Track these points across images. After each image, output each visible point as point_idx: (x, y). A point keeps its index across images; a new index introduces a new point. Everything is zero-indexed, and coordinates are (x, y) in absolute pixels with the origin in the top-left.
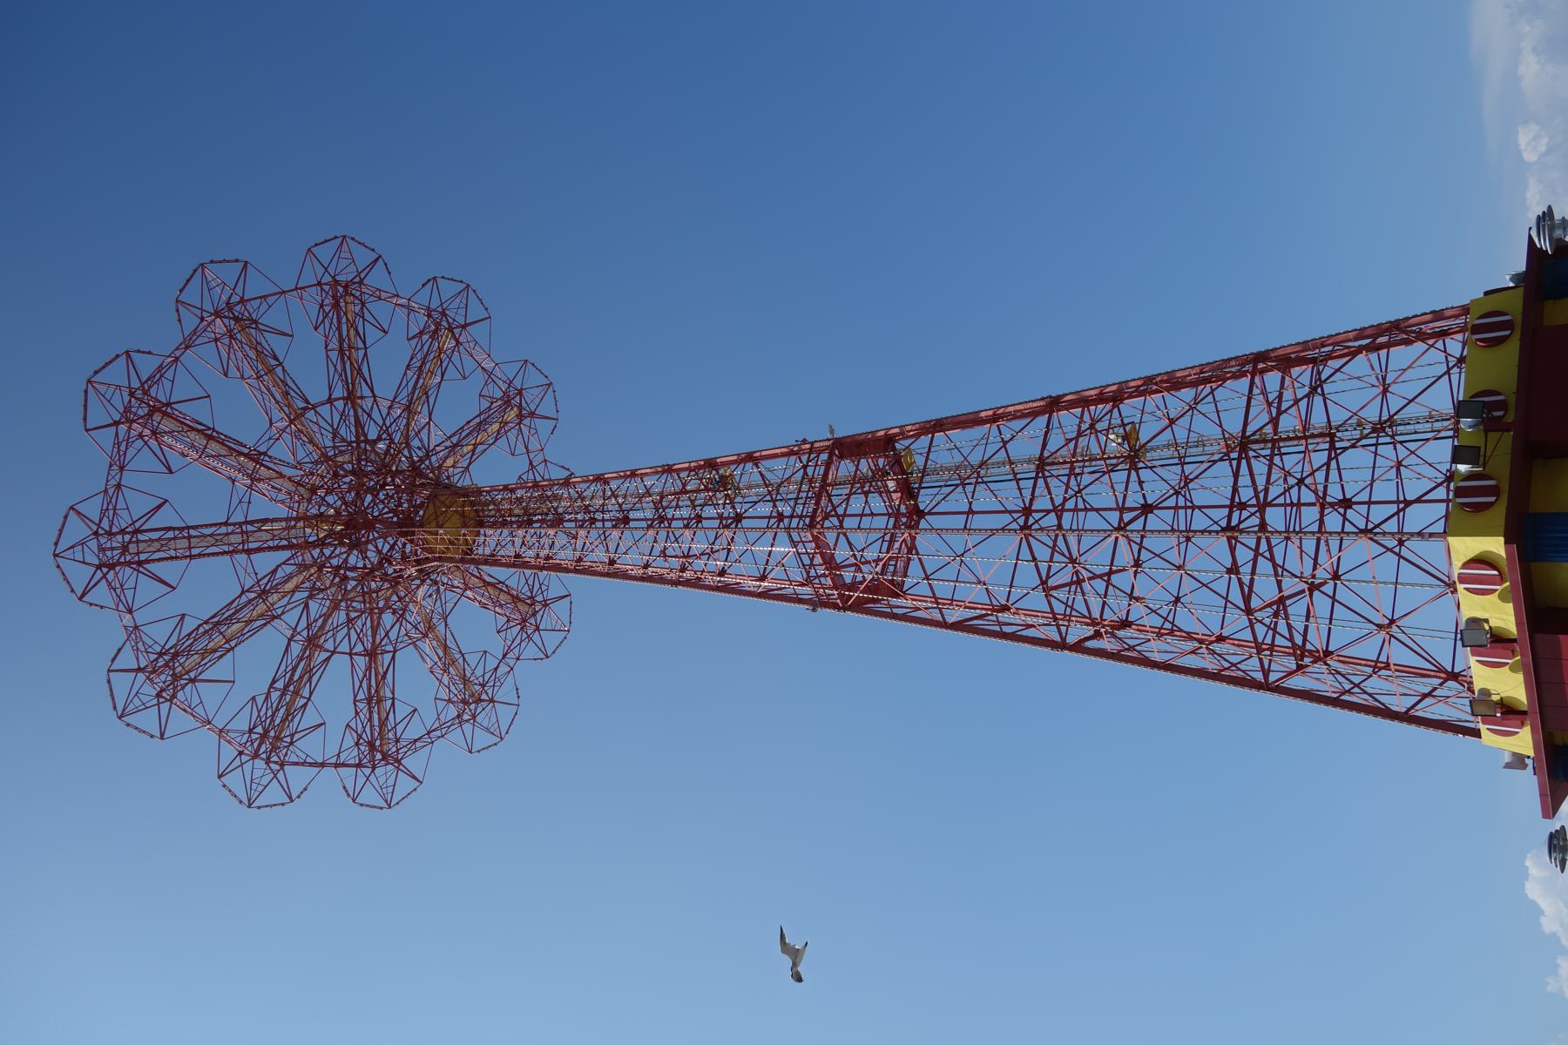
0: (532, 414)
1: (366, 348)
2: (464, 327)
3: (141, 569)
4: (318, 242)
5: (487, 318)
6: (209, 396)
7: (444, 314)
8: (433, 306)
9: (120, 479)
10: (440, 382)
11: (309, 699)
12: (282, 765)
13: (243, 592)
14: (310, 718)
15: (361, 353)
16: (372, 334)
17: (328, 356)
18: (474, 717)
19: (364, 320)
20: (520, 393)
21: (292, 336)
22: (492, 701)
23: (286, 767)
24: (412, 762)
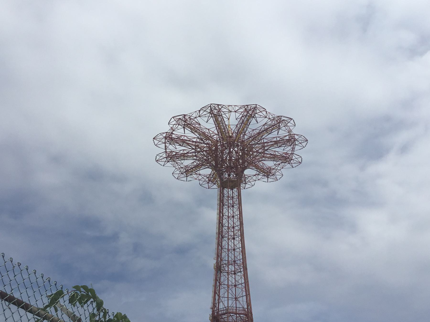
1: (278, 147)
3: (209, 118)
9: (233, 112)
11: (182, 146)
12: (165, 143)
13: (208, 129)
14: (177, 147)
15: (277, 146)
16: (282, 148)
17: (275, 137)
18: (182, 174)
19: (285, 146)
20: (274, 175)
21: (278, 135)
22: (187, 176)
23: (164, 144)
24: (169, 164)
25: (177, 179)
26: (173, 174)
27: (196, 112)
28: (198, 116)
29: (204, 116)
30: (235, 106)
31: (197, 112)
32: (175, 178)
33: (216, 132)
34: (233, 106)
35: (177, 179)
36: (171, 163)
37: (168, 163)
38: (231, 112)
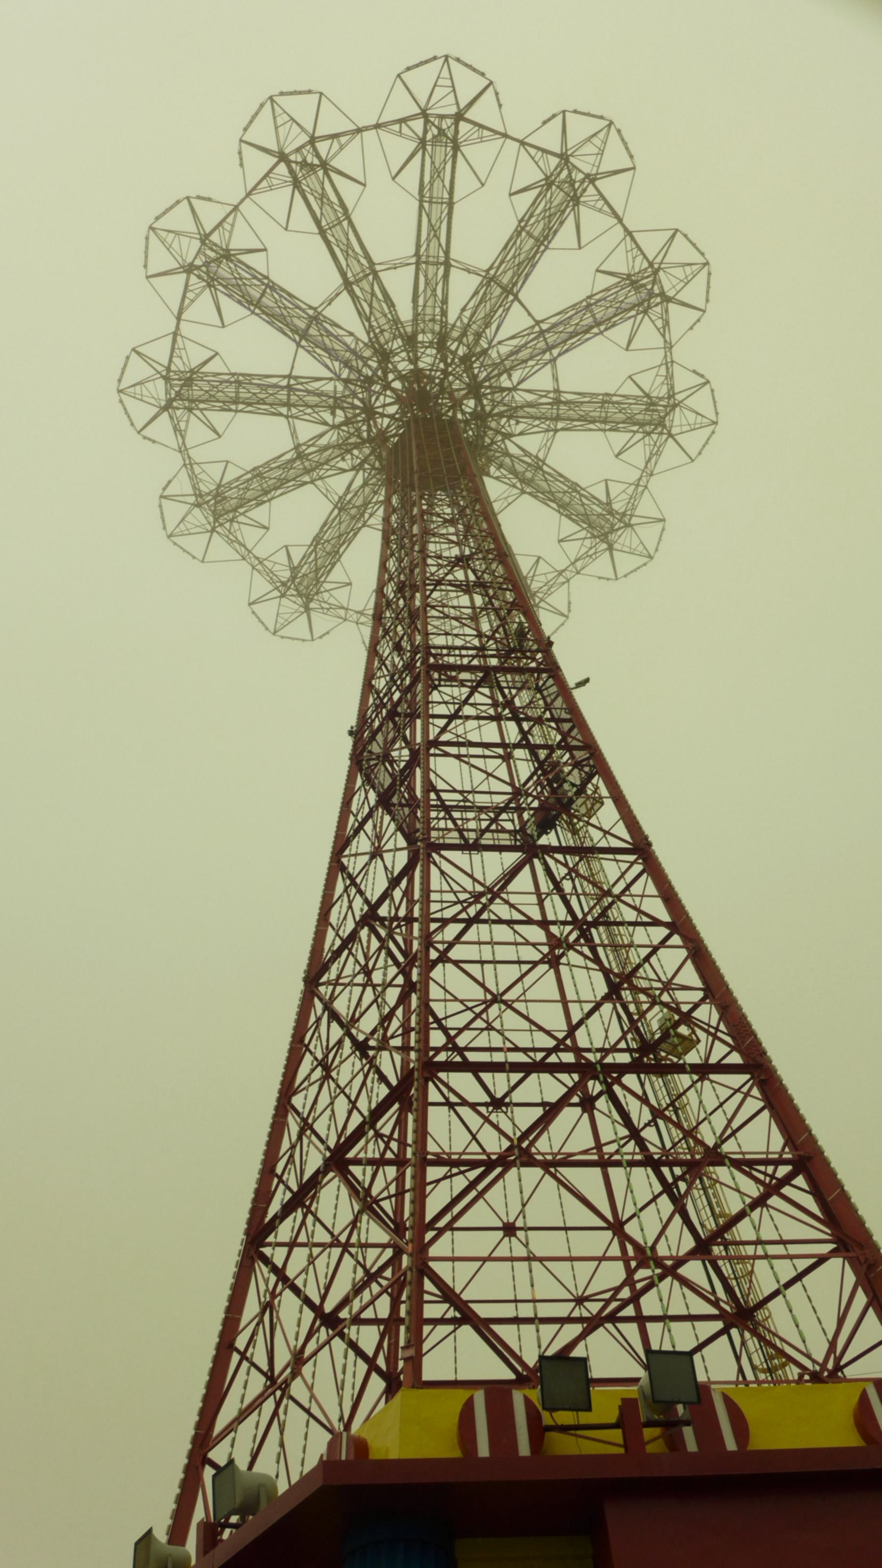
0: (611, 548)
1: (601, 333)
2: (670, 435)
4: (689, 236)
5: (690, 457)
6: (483, 185)
7: (674, 406)
8: (677, 397)
10: (600, 430)
20: (628, 525)
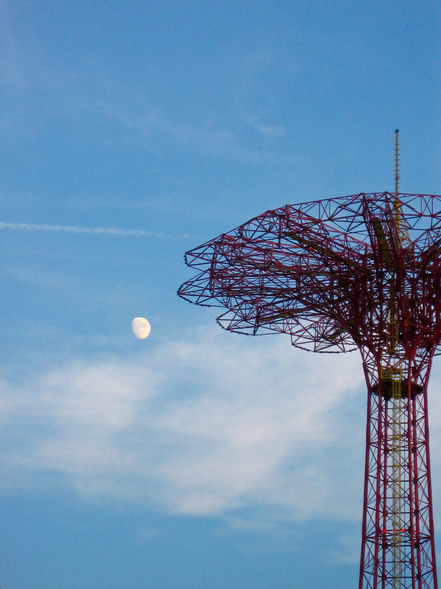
25: (228, 329)
26: (220, 321)
27: (319, 202)
28: (325, 218)
29: (345, 219)
30: (433, 196)
31: (324, 203)
32: (223, 328)
33: (368, 241)
34: (427, 198)
35: (228, 329)
36: (220, 299)
37: (213, 299)
38: (420, 215)
